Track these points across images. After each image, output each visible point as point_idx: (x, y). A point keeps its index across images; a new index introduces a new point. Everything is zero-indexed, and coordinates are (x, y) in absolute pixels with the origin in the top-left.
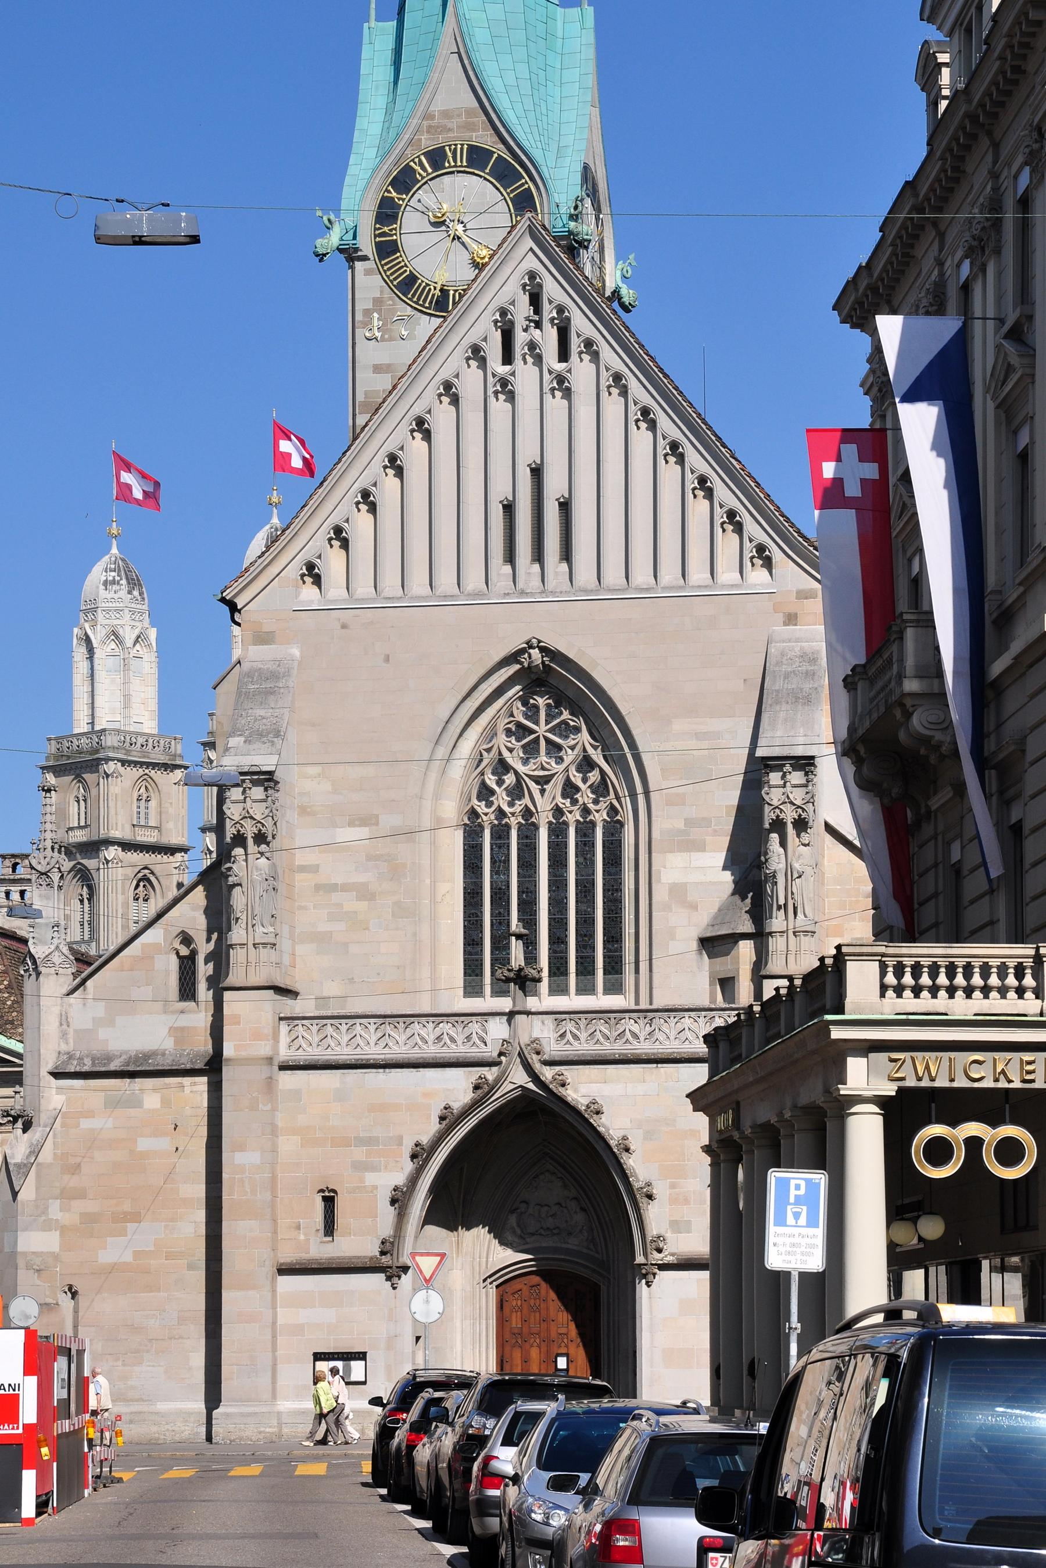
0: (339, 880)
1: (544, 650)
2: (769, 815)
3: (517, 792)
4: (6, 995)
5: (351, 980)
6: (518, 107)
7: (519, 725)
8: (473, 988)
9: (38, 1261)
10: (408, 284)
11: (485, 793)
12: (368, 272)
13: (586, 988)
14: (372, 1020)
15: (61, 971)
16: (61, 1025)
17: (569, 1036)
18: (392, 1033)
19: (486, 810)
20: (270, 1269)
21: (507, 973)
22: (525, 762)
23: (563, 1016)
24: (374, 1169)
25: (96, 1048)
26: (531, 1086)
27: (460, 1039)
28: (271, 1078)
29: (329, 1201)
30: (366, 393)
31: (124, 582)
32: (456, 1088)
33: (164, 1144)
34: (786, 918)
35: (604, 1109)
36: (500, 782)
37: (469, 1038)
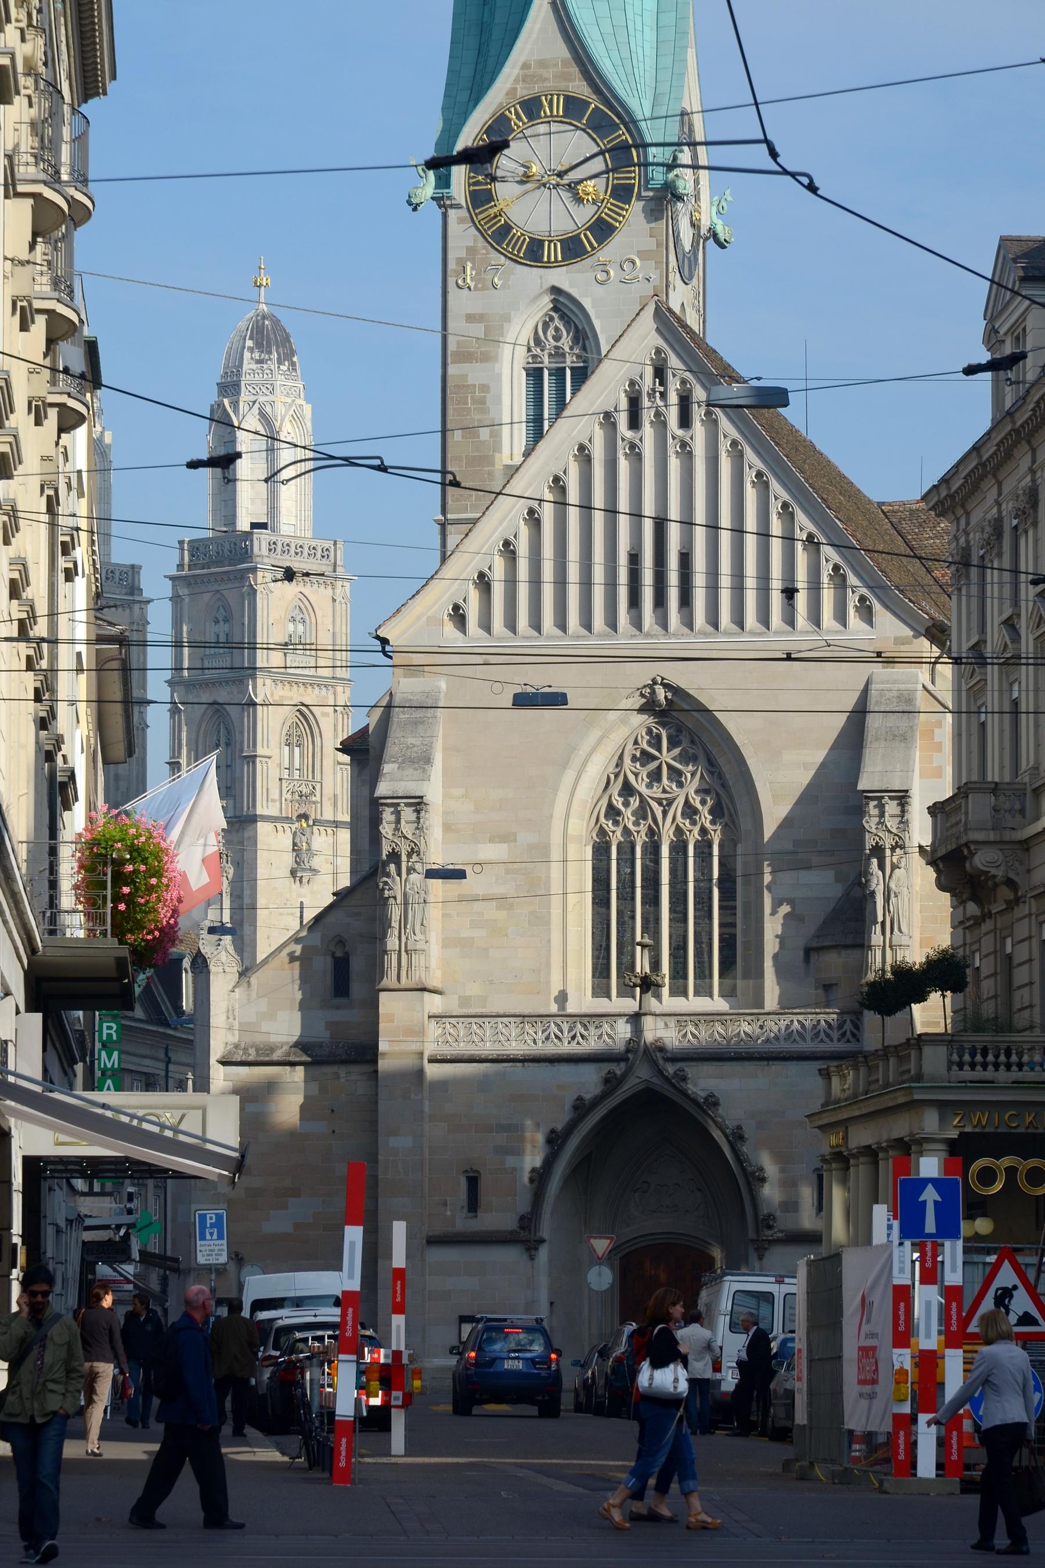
1: (666, 686)
2: (870, 842)
3: (642, 812)
5: (491, 982)
6: (615, 54)
7: (644, 752)
8: (601, 989)
10: (501, 234)
11: (612, 812)
12: (461, 221)
13: (704, 990)
14: (512, 1020)
15: (227, 970)
19: (613, 828)
21: (634, 980)
23: (685, 1018)
25: (259, 1039)
26: (655, 1080)
29: (473, 1182)
34: (883, 933)
35: (721, 1101)
36: (626, 804)
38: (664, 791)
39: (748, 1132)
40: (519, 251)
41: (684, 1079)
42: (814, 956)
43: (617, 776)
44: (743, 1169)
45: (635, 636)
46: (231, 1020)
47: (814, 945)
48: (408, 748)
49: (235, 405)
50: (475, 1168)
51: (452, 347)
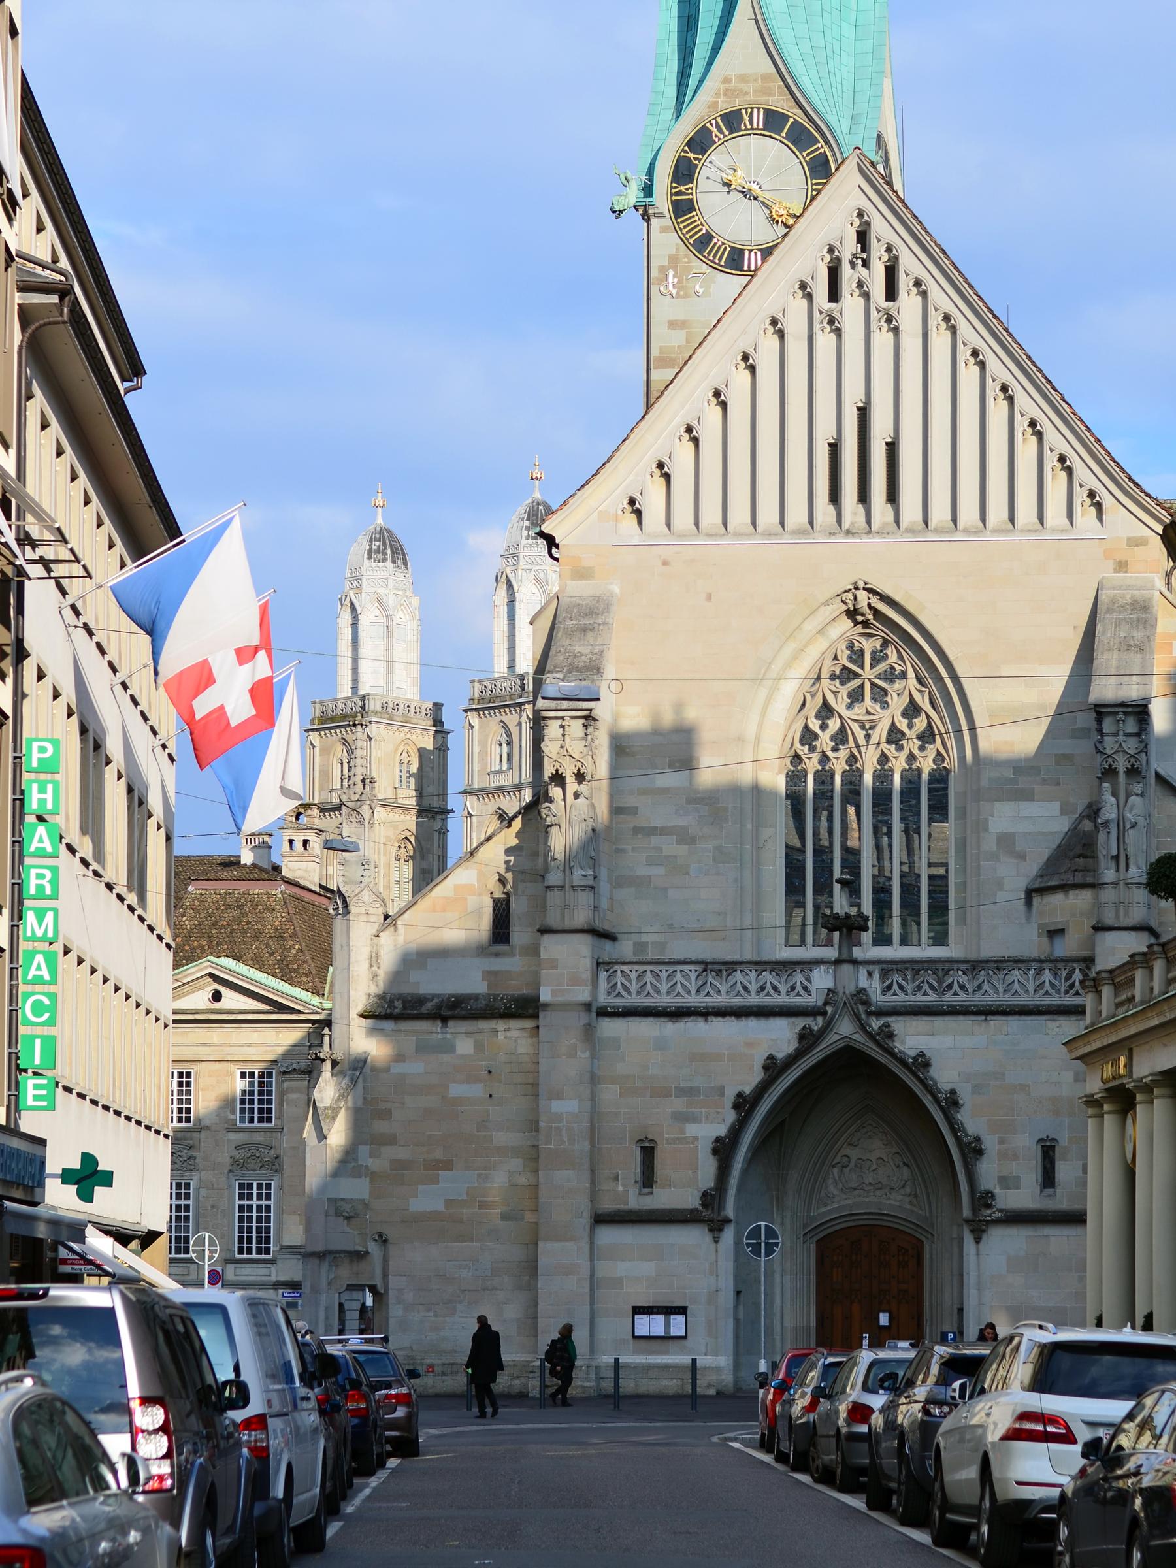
0: (659, 823)
4: (290, 943)
7: (844, 668)
9: (348, 1207)
10: (704, 242)
11: (808, 737)
12: (664, 230)
14: (692, 967)
16: (371, 966)
17: (895, 987)
18: (714, 982)
20: (586, 1220)
22: (850, 707)
24: (694, 1119)
26: (856, 1037)
27: (783, 989)
28: (589, 1025)
29: (648, 1152)
30: (661, 348)
31: (389, 552)
32: (780, 1037)
33: (476, 1091)
34: (1117, 871)
35: (933, 1062)
36: (824, 727)
37: (793, 988)
38: (868, 713)
39: (964, 1096)
40: (720, 259)
41: (891, 1036)
42: (1036, 900)
43: (813, 696)
44: (958, 1140)
45: (834, 534)
46: (375, 968)
47: (1037, 885)
48: (575, 656)
49: (515, 571)
50: (650, 1137)
51: (654, 352)
